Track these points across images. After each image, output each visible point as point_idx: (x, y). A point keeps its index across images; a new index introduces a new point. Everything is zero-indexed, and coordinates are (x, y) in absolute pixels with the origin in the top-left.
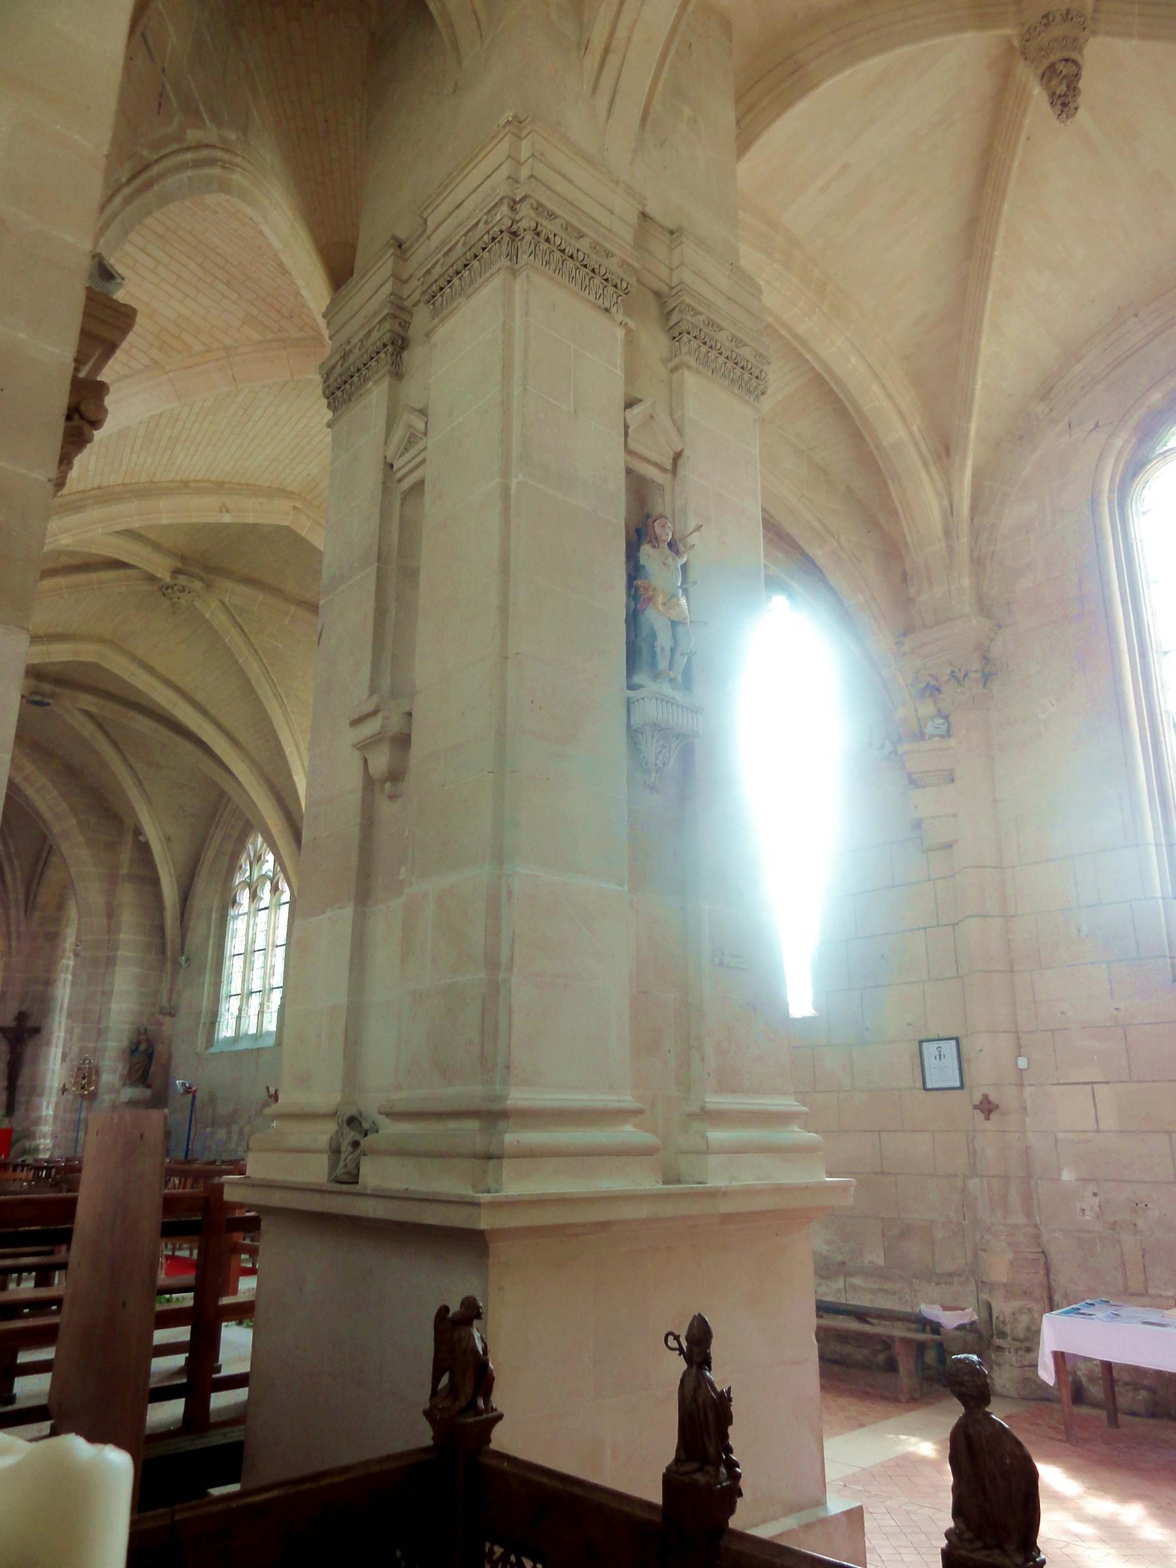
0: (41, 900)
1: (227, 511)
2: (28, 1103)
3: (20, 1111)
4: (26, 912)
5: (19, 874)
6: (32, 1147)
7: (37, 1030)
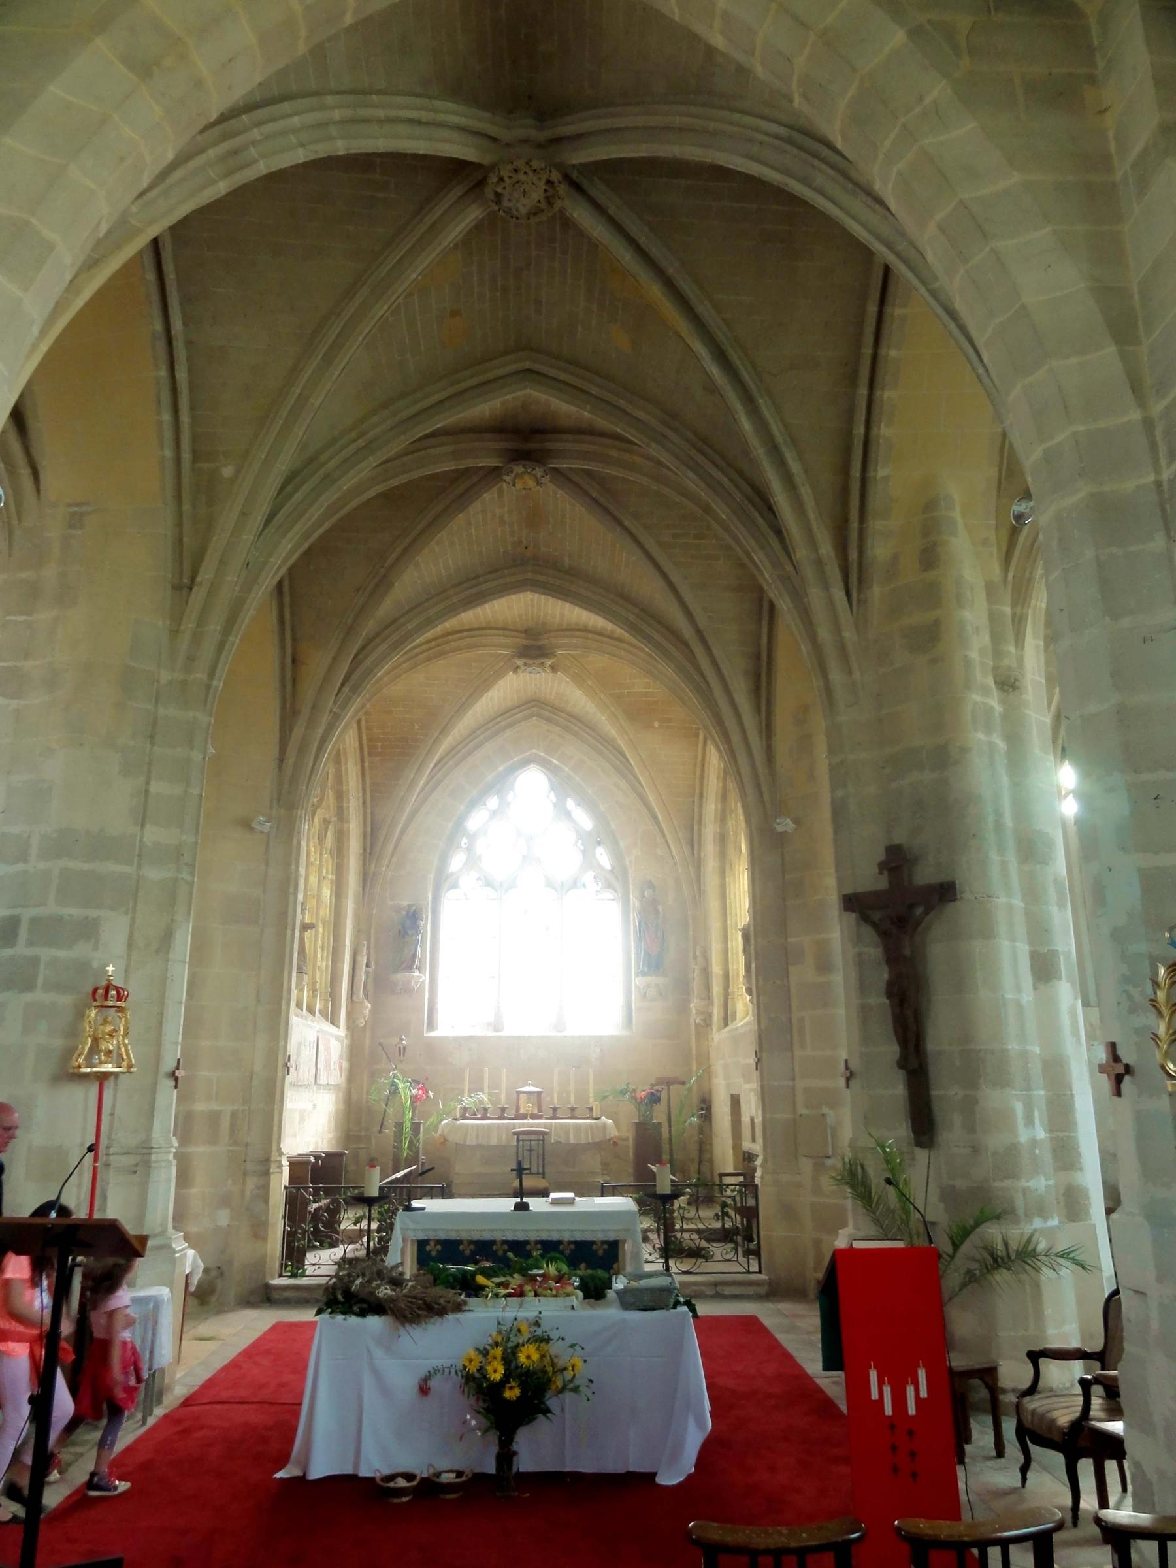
0: (880, 551)
2: (970, 1105)
3: (951, 1134)
6: (1014, 1246)
7: (946, 892)
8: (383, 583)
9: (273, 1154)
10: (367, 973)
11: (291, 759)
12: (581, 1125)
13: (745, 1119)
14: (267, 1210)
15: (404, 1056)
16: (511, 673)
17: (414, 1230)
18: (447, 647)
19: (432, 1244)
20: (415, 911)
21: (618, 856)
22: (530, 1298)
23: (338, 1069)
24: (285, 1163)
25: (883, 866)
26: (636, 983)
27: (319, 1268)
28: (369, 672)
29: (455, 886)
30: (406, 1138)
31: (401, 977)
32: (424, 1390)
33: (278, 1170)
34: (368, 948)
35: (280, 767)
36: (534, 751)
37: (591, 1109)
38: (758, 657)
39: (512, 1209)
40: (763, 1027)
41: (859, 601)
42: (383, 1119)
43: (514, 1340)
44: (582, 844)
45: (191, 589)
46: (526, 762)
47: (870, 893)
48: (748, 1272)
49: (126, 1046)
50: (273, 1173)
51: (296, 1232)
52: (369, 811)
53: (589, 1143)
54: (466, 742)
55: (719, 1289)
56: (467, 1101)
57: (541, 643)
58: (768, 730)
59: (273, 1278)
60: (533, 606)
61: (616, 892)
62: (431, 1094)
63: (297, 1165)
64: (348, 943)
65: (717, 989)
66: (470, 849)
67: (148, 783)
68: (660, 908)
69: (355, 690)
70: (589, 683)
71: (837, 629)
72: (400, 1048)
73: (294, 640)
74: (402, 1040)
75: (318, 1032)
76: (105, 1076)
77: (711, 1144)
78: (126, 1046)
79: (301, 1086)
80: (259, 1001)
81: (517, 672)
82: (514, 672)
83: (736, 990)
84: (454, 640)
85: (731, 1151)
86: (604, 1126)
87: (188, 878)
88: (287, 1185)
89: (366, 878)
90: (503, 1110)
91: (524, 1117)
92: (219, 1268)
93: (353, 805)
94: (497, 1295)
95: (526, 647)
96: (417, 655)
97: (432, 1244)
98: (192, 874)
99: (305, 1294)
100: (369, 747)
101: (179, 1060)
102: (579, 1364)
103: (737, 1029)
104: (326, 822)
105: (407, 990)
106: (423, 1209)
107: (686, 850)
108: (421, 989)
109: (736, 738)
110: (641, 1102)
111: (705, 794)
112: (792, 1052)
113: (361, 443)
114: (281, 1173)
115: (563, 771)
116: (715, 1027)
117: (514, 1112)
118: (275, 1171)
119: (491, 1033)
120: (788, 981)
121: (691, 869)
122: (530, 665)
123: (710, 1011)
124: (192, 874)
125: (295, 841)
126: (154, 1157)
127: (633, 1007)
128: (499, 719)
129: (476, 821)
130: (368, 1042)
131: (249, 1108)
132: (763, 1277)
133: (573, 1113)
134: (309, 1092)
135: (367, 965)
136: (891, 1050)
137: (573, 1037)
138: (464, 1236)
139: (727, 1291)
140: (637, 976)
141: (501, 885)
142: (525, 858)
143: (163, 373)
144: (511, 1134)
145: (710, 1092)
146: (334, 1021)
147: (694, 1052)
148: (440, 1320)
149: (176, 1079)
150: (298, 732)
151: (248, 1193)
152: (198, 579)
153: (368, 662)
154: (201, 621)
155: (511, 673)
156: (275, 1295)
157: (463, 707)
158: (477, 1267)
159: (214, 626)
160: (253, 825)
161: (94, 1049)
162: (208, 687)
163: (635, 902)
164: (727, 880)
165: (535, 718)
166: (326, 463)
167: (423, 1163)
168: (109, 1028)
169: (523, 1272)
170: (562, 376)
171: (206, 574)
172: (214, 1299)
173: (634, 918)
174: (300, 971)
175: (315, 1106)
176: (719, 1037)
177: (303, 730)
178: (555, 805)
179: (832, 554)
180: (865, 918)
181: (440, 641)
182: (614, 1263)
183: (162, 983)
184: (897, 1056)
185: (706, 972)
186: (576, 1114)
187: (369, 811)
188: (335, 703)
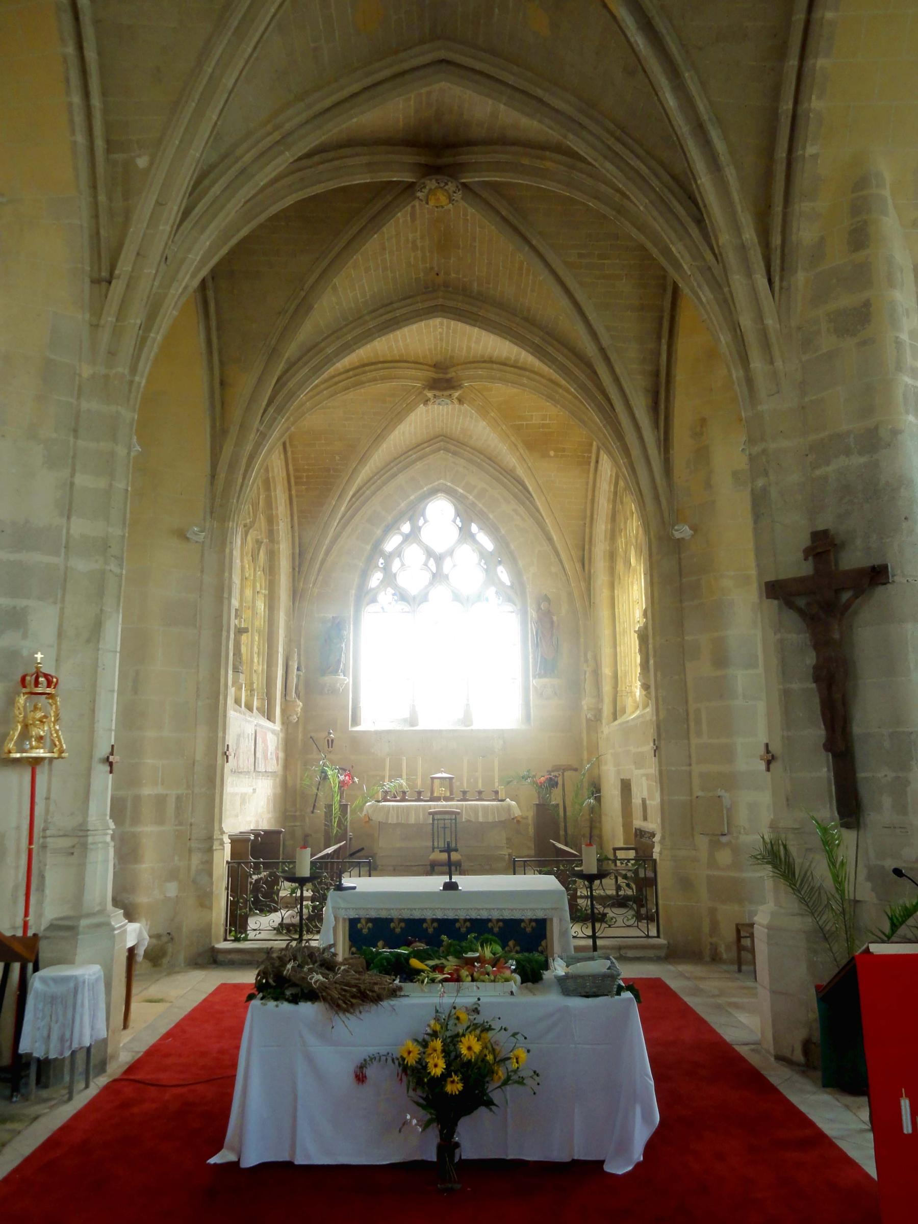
4: (770, 282)
5: (730, 173)
8: (303, 307)
9: (215, 832)
10: (298, 676)
11: (222, 476)
12: (488, 806)
13: (636, 801)
14: (212, 884)
15: (332, 747)
16: (422, 405)
17: (346, 909)
18: (363, 378)
19: (363, 922)
20: (339, 622)
21: (517, 574)
22: (467, 984)
23: (274, 757)
24: (227, 840)
25: (807, 552)
26: (533, 685)
27: (260, 933)
28: (292, 395)
29: (374, 600)
30: (335, 818)
31: (328, 679)
32: (360, 1077)
33: (222, 847)
34: (299, 655)
35: (212, 484)
36: (442, 481)
37: (497, 792)
38: (657, 374)
39: (442, 888)
40: (661, 717)
41: (781, 288)
42: (315, 801)
43: (452, 1030)
44: (485, 563)
45: (110, 283)
46: (434, 492)
47: (794, 580)
48: (648, 936)
49: (57, 732)
50: (216, 850)
51: (238, 902)
52: (296, 534)
53: (496, 821)
54: (382, 472)
55: (623, 952)
56: (388, 785)
57: (449, 376)
58: (665, 444)
59: (218, 942)
60: (441, 340)
61: (515, 605)
62: (356, 780)
63: (238, 842)
64: (281, 650)
65: (607, 688)
66: (386, 569)
67: (72, 475)
68: (555, 618)
69: (280, 410)
70: (492, 414)
71: (760, 317)
72: (328, 741)
73: (222, 363)
74: (330, 733)
75: (256, 726)
76: (38, 761)
77: (600, 822)
79: (241, 773)
80: (198, 696)
81: (427, 404)
82: (424, 405)
83: (624, 689)
84: (371, 371)
85: (621, 828)
86: (509, 805)
87: (117, 570)
88: (229, 860)
89: (296, 594)
90: (419, 793)
91: (438, 799)
92: (169, 934)
93: (283, 528)
94: (433, 981)
95: (435, 381)
96: (336, 384)
97: (363, 922)
98: (121, 568)
99: (248, 957)
100: (296, 478)
101: (113, 746)
102: (523, 1055)
103: (628, 722)
104: (259, 543)
105: (334, 691)
106: (354, 888)
107: (578, 566)
108: (346, 690)
109: (636, 452)
110: (541, 786)
111: (595, 516)
112: (689, 739)
113: (277, 136)
114: (224, 849)
115: (468, 498)
116: (604, 721)
117: (429, 794)
118: (218, 848)
119: (407, 728)
120: (685, 675)
121: (582, 584)
122: (439, 397)
123: (600, 707)
124: (121, 566)
125: (227, 551)
126: (90, 839)
127: (531, 705)
128: (410, 453)
129: (392, 543)
130: (300, 736)
131: (193, 792)
132: (662, 941)
133: (480, 796)
134: (249, 778)
135: (298, 669)
136: (817, 733)
137: (479, 731)
138: (395, 915)
139: (630, 954)
140: (534, 677)
141: (414, 598)
142: (434, 575)
143: (70, 50)
144: (427, 814)
145: (599, 777)
146: (270, 717)
147: (585, 743)
148: (374, 1007)
149: (111, 764)
150: (228, 449)
151: (193, 868)
152: (117, 272)
153: (291, 385)
154: (121, 314)
155: (422, 405)
156: (220, 957)
157: (379, 438)
158: (410, 949)
159: (135, 319)
160: (188, 536)
161: (25, 735)
162: (131, 383)
163: (532, 613)
164: (616, 592)
165: (442, 452)
166: (242, 157)
167: (351, 839)
168: (39, 715)
169: (458, 954)
170: (478, 66)
171: (124, 267)
172: (165, 961)
173: (532, 627)
174: (236, 670)
175: (254, 790)
176: (608, 729)
177: (233, 447)
178: (460, 529)
179: (756, 240)
180: (789, 604)
181: (356, 371)
182: (542, 940)
183: (93, 671)
184: (823, 741)
185: (597, 673)
186: (483, 796)
187: (296, 534)
188: (261, 421)
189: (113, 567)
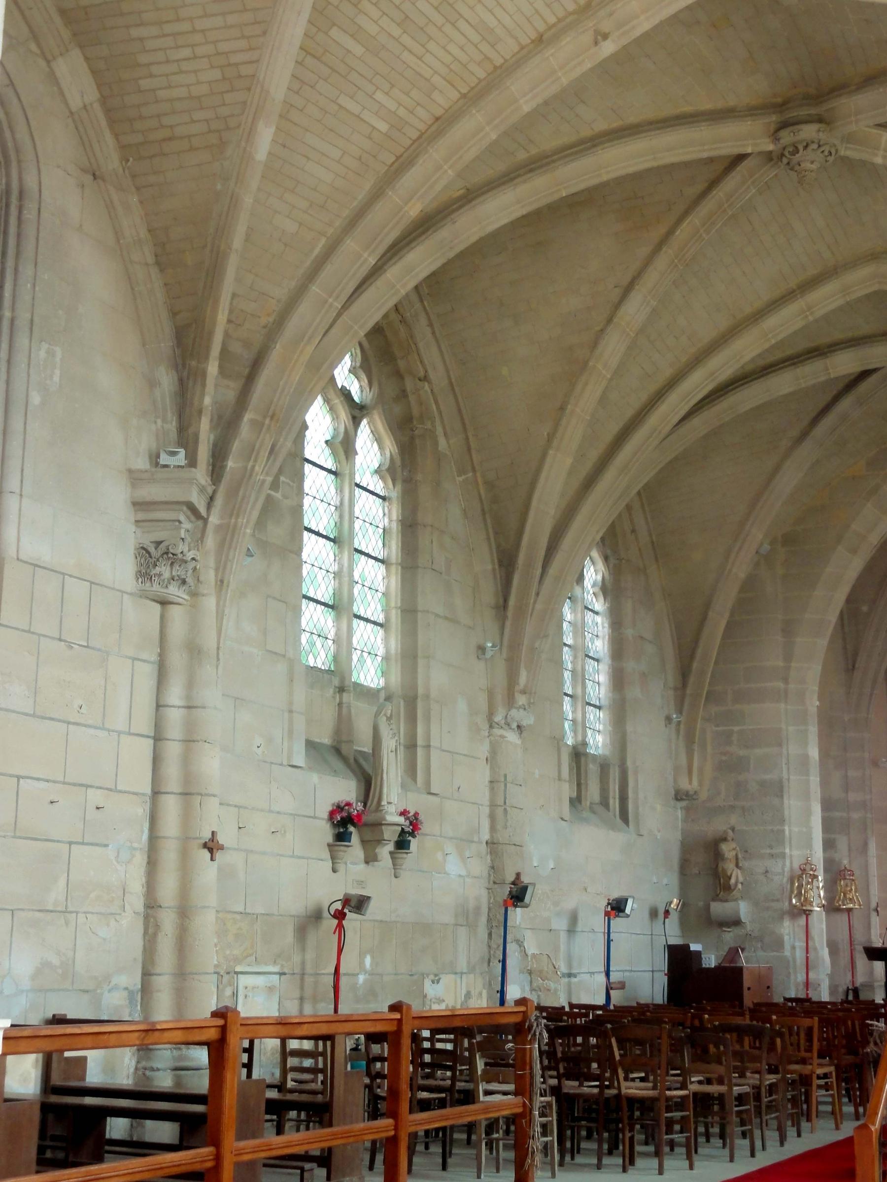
1: (605, 37)
49: (857, 896)
78: (857, 896)
152: (857, 666)
168: (849, 889)
183: (866, 867)
189: (869, 815)
